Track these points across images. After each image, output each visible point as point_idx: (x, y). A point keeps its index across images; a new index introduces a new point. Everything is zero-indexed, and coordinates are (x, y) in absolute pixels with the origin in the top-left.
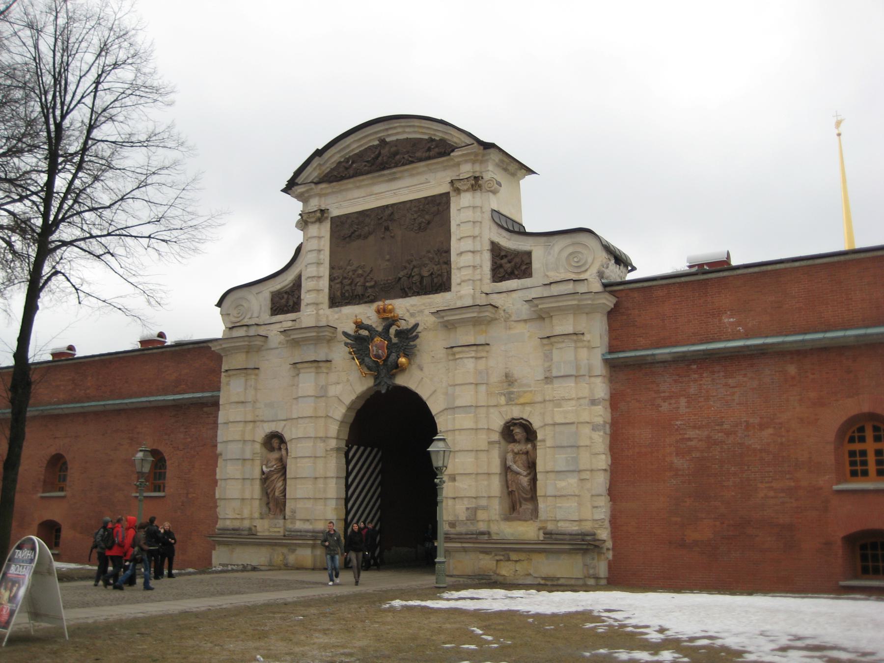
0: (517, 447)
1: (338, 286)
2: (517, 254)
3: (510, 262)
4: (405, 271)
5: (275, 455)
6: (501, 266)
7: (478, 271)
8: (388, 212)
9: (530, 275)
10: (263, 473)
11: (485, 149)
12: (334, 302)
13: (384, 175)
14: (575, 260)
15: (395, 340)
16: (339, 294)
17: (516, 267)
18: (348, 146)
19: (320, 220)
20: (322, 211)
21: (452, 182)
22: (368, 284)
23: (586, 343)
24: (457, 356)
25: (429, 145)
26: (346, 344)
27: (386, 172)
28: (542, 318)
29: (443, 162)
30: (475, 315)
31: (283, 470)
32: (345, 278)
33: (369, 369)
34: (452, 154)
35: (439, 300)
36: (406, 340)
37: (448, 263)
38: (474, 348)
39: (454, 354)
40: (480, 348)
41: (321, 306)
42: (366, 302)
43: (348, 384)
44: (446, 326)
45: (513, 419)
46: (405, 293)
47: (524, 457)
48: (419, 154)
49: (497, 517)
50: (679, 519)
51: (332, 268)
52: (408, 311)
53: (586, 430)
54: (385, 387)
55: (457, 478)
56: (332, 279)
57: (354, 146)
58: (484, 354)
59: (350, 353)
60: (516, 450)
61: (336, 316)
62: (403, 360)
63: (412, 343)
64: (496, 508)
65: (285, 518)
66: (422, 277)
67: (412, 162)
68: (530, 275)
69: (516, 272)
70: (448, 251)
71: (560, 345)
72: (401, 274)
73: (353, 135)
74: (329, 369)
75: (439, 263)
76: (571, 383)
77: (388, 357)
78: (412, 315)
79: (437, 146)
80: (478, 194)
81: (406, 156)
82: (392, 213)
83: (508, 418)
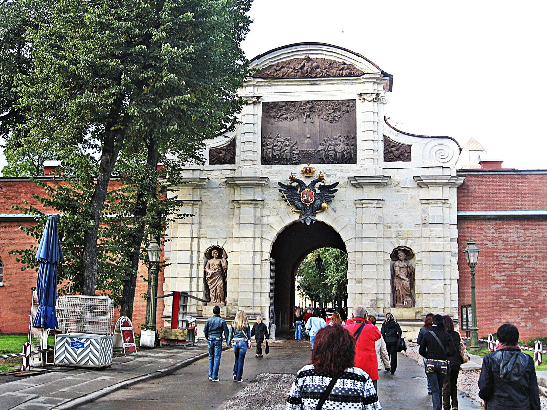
0: (402, 264)
1: (270, 150)
2: (402, 145)
3: (397, 150)
4: (324, 147)
5: (215, 262)
6: (391, 152)
7: (376, 153)
8: (309, 106)
9: (410, 160)
10: (205, 273)
11: (384, 77)
12: (265, 160)
13: (309, 81)
14: (441, 154)
15: (318, 191)
16: (270, 155)
17: (401, 154)
18: (279, 56)
19: (254, 103)
20: (258, 98)
21: (360, 95)
22: (294, 152)
23: (448, 205)
24: (364, 206)
25: (342, 66)
26: (280, 191)
27: (310, 79)
28: (420, 186)
29: (353, 80)
30: (380, 181)
31: (223, 272)
32: (276, 146)
33: (297, 208)
34: (362, 76)
35: (348, 169)
36: (328, 192)
37: (355, 145)
38: (376, 202)
39: (362, 204)
40: (380, 201)
41: (255, 162)
42: (292, 164)
43: (281, 216)
44: (355, 186)
45: (400, 246)
46: (322, 161)
47: (405, 270)
48: (334, 71)
49: (389, 306)
50: (498, 308)
51: (263, 137)
52: (325, 173)
53: (448, 256)
54: (310, 221)
55: (363, 281)
56: (263, 145)
57: (284, 57)
58: (381, 206)
59: (283, 197)
60: (401, 266)
61: (268, 170)
62: (324, 205)
63: (330, 194)
64: (389, 298)
65: (225, 305)
66: (336, 152)
67: (329, 76)
68: (410, 160)
69: (402, 157)
70: (355, 138)
71: (434, 205)
72: (320, 148)
73: (285, 49)
74: (263, 206)
75: (348, 145)
76: (439, 228)
77: (315, 201)
78: (328, 176)
79: (348, 68)
80: (376, 104)
81: (325, 71)
82: (312, 107)
83: (397, 246)
